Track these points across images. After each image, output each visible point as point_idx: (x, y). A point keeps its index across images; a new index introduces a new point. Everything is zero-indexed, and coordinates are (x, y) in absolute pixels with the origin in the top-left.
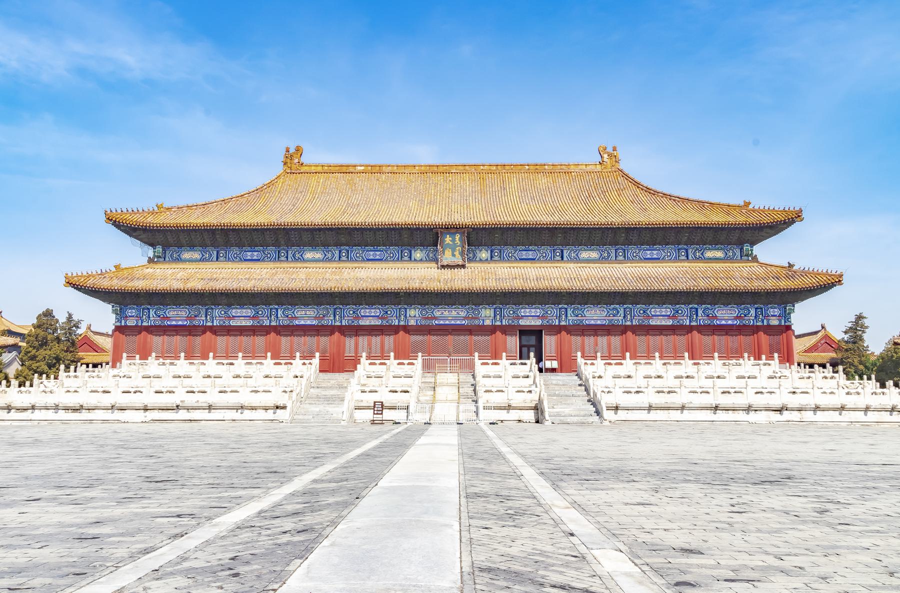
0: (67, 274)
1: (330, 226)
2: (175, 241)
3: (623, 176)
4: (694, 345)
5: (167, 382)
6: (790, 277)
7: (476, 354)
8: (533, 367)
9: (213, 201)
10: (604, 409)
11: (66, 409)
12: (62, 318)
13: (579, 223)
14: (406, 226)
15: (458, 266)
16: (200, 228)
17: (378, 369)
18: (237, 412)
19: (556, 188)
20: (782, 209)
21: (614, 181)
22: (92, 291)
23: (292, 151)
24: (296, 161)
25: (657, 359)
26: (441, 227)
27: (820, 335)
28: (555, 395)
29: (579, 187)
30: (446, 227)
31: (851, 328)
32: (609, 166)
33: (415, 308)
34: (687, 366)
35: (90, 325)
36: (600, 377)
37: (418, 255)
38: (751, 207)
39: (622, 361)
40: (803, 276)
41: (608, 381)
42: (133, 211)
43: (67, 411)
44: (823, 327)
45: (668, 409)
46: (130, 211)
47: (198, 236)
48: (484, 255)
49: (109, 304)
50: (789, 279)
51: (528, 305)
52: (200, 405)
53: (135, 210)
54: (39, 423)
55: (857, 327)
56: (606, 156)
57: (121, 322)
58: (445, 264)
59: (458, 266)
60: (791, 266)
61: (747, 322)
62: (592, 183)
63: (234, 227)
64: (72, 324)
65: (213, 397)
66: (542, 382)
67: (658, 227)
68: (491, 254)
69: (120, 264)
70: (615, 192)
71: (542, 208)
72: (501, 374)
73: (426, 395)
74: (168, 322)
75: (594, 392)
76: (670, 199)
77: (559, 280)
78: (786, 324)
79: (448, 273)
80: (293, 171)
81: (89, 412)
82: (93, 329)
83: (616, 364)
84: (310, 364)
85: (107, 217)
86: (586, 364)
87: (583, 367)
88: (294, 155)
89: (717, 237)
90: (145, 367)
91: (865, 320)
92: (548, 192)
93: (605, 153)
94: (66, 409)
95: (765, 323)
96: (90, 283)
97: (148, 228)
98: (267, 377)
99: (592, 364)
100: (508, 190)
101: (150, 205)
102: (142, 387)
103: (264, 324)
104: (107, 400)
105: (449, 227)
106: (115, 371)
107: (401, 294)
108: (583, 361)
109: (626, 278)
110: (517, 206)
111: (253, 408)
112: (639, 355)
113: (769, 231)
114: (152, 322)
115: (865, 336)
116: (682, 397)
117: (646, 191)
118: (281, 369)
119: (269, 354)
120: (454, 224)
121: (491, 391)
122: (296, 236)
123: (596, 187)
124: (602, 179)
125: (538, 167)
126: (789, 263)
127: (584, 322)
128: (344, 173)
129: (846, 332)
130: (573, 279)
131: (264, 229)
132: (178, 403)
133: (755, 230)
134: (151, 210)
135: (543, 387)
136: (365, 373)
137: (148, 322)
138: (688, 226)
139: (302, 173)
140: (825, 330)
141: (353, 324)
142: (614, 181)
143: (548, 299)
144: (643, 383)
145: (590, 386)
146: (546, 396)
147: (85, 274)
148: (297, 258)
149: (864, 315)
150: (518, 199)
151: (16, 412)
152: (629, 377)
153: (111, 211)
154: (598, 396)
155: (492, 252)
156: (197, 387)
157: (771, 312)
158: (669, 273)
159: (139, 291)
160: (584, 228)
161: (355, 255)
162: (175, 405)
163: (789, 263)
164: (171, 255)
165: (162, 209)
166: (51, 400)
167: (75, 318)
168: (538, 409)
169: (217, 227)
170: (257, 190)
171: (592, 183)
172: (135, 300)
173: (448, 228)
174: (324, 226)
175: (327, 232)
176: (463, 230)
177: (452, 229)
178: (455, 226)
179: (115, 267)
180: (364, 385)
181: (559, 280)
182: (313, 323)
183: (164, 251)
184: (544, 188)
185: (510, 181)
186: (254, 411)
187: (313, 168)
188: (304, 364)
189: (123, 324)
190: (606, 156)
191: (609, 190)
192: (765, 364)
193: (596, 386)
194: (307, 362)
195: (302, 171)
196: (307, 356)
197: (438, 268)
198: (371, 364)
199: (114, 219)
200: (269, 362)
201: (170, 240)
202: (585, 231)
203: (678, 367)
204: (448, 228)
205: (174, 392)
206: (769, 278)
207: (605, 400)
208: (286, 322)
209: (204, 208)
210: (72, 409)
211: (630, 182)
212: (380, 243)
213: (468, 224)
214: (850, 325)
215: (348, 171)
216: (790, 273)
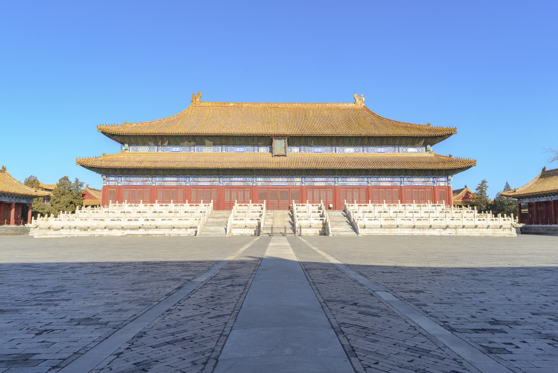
0: (77, 158)
1: (217, 135)
2: (135, 141)
3: (366, 110)
4: (402, 196)
5: (134, 215)
6: (450, 162)
7: (294, 201)
8: (322, 207)
10: (359, 228)
11: (81, 229)
12: (73, 181)
13: (344, 134)
14: (256, 135)
15: (283, 155)
16: (148, 134)
17: (244, 208)
18: (171, 230)
19: (332, 116)
21: (362, 112)
22: (91, 167)
23: (196, 95)
24: (198, 100)
25: (385, 203)
26: (274, 135)
27: (464, 190)
28: (333, 221)
29: (344, 115)
30: (277, 135)
31: (479, 187)
33: (261, 177)
34: (399, 207)
35: (88, 185)
36: (356, 212)
37: (262, 150)
38: (431, 126)
39: (367, 204)
40: (457, 162)
41: (360, 214)
43: (81, 230)
44: (466, 187)
45: (391, 228)
46: (111, 125)
47: (147, 139)
49: (100, 174)
50: (450, 163)
51: (319, 175)
52: (152, 227)
53: (113, 125)
54: (66, 236)
55: (482, 187)
57: (106, 184)
59: (283, 155)
60: (450, 156)
61: (429, 184)
62: (350, 114)
63: (166, 135)
64: (78, 184)
65: (159, 222)
66: (327, 215)
67: (384, 136)
68: (300, 150)
69: (105, 153)
70: (362, 118)
71: (325, 126)
72: (306, 211)
73: (268, 221)
74: (132, 184)
75: (353, 219)
76: (390, 122)
77: (334, 163)
78: (448, 185)
79: (277, 159)
80: (196, 105)
81: (93, 231)
82: (89, 187)
83: (364, 206)
84: (208, 205)
85: (98, 128)
86: (349, 205)
87: (347, 207)
89: (414, 142)
90: (121, 207)
91: (487, 184)
92: (328, 118)
94: (81, 229)
95: (438, 185)
96: (89, 164)
98: (185, 212)
99: (352, 206)
100: (308, 117)
102: (121, 218)
104: (103, 224)
105: (278, 135)
106: (106, 210)
107: (254, 170)
108: (347, 204)
109: (368, 162)
110: (312, 125)
111: (179, 228)
112: (388, 201)
113: (439, 138)
114: (123, 184)
115: (487, 192)
116: (398, 222)
117: (378, 118)
118: (193, 208)
119: (187, 201)
120: (281, 134)
122: (199, 139)
123: (353, 116)
124: (356, 111)
126: (449, 155)
127: (347, 184)
129: (477, 190)
130: (341, 162)
131: (182, 136)
132: (140, 226)
133: (433, 138)
135: (328, 217)
136: (236, 211)
137: (121, 184)
138: (399, 136)
139: (201, 106)
140: (467, 188)
141: (229, 185)
142: (362, 112)
143: (329, 172)
144: (377, 215)
145: (351, 217)
146: (329, 221)
148: (199, 151)
149: (486, 181)
150: (313, 121)
151: (54, 231)
152: (370, 212)
153: (100, 125)
154: (356, 221)
155: (300, 148)
156: (150, 218)
157: (441, 179)
158: (390, 160)
159: (116, 168)
160: (347, 137)
161: (229, 150)
162: (138, 227)
163: (449, 155)
164: (198, 149)
165: (127, 124)
166: (73, 224)
167: (80, 181)
168: (325, 228)
169: (157, 134)
171: (350, 114)
172: (114, 172)
173: (277, 136)
174: (214, 135)
175: (215, 137)
176: (285, 137)
177: (280, 137)
178: (281, 135)
180: (237, 216)
181: (334, 163)
182: (208, 185)
184: (326, 116)
185: (309, 112)
186: (180, 230)
187: (207, 104)
188: (205, 206)
189: (107, 185)
190: (357, 100)
191: (359, 117)
192: (438, 206)
193: (354, 216)
194: (207, 204)
196: (207, 201)
197: (272, 157)
198: (240, 206)
200: (187, 205)
201: (132, 141)
202: (347, 138)
203: (395, 207)
204: (277, 136)
206: (440, 162)
207: (359, 224)
209: (150, 124)
211: (370, 113)
212: (242, 144)
213: (288, 134)
214: (479, 186)
216: (450, 160)
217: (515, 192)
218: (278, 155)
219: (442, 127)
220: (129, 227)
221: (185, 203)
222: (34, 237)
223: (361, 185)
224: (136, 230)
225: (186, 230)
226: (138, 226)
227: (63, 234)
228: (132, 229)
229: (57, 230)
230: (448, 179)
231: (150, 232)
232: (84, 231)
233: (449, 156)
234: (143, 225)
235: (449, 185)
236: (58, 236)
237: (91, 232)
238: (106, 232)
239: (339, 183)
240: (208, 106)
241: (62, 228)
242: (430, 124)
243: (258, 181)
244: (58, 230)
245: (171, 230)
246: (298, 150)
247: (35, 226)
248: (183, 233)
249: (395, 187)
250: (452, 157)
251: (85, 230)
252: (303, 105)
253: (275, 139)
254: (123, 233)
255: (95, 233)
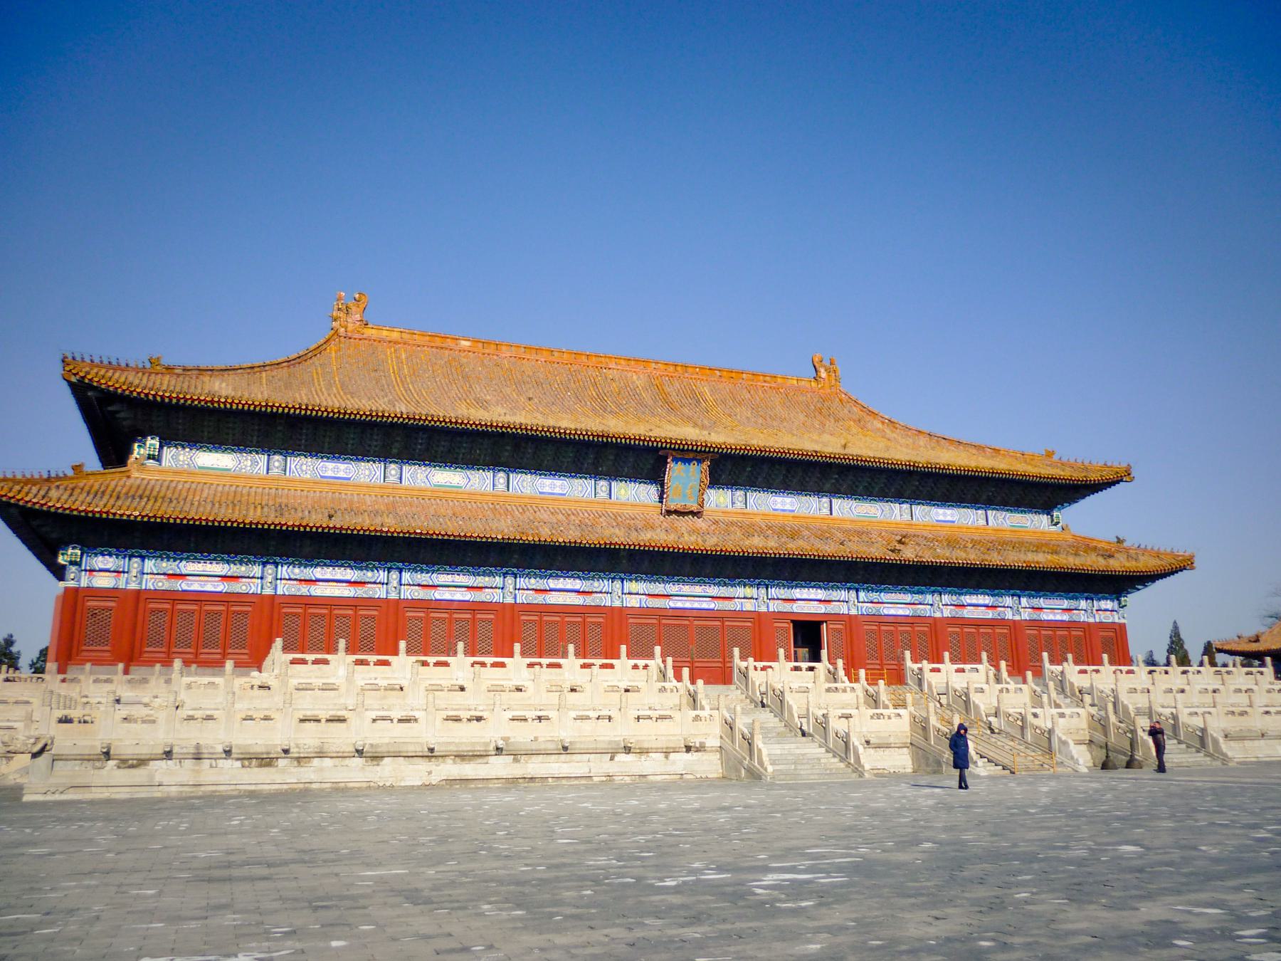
9: (237, 367)
18: (612, 759)
20: (1101, 463)
24: (358, 317)
32: (827, 385)
37: (623, 491)
38: (1055, 458)
42: (110, 362)
43: (246, 763)
46: (106, 362)
48: (722, 499)
52: (543, 747)
56: (822, 370)
57: (79, 581)
58: (672, 507)
60: (1119, 541)
65: (565, 731)
80: (349, 334)
88: (354, 309)
93: (822, 366)
97: (167, 400)
101: (138, 357)
103: (377, 597)
107: (622, 553)
121: (588, 718)
125: (733, 375)
126: (1117, 538)
128: (437, 348)
134: (141, 366)
147: (19, 476)
151: (119, 767)
163: (1117, 538)
165: (158, 368)
170: (299, 357)
173: (683, 450)
177: (688, 453)
179: (75, 468)
182: (467, 598)
183: (161, 447)
186: (643, 757)
187: (385, 333)
188: (635, 667)
190: (822, 370)
194: (641, 663)
195: (364, 336)
199: (82, 374)
205: (416, 720)
208: (416, 594)
210: (256, 758)
215: (444, 345)
217: (1257, 640)
218: (677, 512)
219: (1105, 465)
220: (453, 748)
221: (512, 657)
222: (26, 798)
223: (919, 613)
224: (480, 760)
225: (667, 757)
226: (487, 744)
227: (166, 781)
228: (461, 757)
229: (132, 766)
230: (1120, 604)
231: (534, 767)
232: (260, 766)
233: (1116, 540)
234: (506, 739)
235: (1122, 621)
236: (143, 794)
237: (293, 770)
238: (356, 773)
239: (862, 608)
240: (390, 342)
241: (168, 755)
242: (1053, 453)
243: (630, 593)
244: (142, 762)
245: (612, 759)
246: (729, 500)
247: (36, 749)
248: (659, 771)
249: (1002, 622)
250: (1125, 544)
251: (266, 761)
252: (679, 368)
253: (676, 460)
254: (430, 773)
255: (313, 777)
